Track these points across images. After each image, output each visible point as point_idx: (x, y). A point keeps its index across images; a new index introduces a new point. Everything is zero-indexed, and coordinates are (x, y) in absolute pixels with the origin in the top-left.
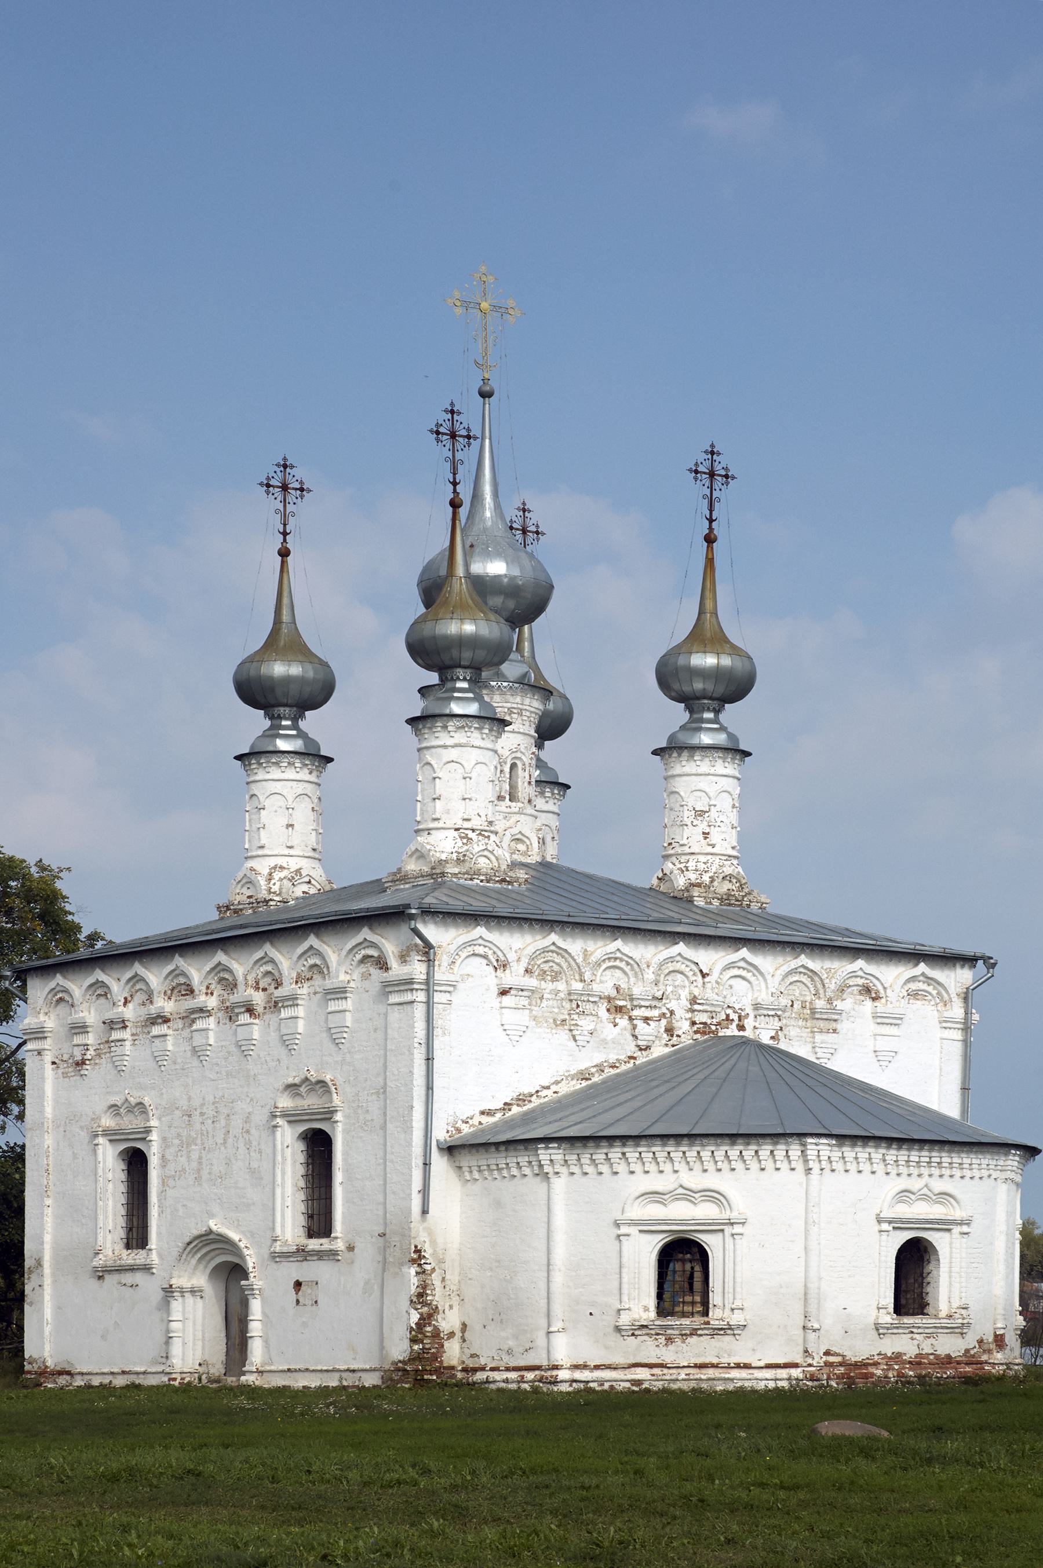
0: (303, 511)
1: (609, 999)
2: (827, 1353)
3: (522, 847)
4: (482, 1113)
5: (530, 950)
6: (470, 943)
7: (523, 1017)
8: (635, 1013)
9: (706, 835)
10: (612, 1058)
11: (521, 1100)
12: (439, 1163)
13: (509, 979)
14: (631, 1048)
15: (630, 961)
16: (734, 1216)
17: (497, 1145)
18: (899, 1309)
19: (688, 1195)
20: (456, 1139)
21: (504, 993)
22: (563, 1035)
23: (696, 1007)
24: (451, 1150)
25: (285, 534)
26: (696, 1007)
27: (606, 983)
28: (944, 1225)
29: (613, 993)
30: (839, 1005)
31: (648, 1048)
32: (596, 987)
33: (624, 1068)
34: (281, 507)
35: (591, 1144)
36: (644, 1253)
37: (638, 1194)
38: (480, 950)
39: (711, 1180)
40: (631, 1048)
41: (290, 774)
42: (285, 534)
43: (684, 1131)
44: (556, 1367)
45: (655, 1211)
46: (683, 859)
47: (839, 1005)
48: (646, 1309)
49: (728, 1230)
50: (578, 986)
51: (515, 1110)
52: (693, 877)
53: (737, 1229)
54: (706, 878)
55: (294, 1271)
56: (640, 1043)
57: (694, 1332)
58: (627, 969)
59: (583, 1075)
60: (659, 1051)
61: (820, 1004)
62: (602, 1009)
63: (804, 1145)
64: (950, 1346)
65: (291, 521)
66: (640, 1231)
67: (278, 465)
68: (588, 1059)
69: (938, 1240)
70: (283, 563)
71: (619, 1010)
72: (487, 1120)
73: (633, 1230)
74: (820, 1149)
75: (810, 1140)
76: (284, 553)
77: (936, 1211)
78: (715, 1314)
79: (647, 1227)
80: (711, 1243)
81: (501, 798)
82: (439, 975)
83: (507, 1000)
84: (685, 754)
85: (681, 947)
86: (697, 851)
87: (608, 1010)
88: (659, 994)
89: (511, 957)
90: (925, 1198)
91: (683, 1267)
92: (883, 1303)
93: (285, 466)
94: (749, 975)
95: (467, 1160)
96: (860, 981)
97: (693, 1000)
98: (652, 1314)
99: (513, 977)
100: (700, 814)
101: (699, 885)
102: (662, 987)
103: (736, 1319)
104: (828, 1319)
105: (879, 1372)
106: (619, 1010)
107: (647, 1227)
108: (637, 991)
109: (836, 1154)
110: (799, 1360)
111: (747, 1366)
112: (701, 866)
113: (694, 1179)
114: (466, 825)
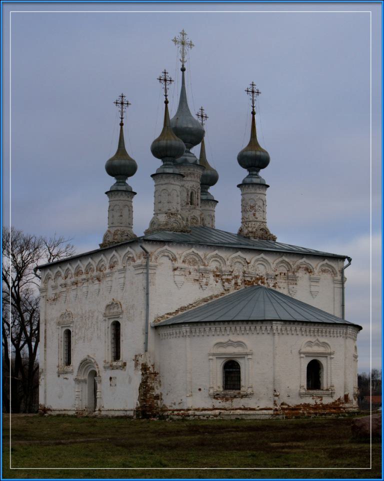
0: (127, 110)
1: (214, 272)
2: (282, 404)
3: (195, 221)
4: (168, 314)
5: (184, 254)
6: (163, 252)
7: (182, 278)
8: (224, 277)
9: (254, 215)
10: (216, 293)
11: (182, 309)
12: (151, 333)
13: (176, 265)
14: (222, 290)
15: (221, 258)
16: (248, 351)
17: (169, 325)
18: (310, 387)
19: (230, 344)
20: (157, 324)
21: (175, 269)
22: (197, 286)
23: (246, 275)
24: (156, 328)
25: (122, 118)
26: (246, 275)
27: (213, 266)
28: (325, 355)
29: (215, 270)
30: (297, 274)
31: (228, 290)
32: (208, 268)
33: (220, 297)
34: (121, 110)
35: (199, 325)
36: (218, 367)
37: (214, 344)
38: (166, 254)
39: (240, 338)
40: (222, 290)
41: (122, 198)
42: (122, 118)
43: (230, 319)
44: (188, 410)
45: (222, 350)
46: (247, 223)
47: (297, 274)
48: (219, 387)
49: (246, 357)
50: (202, 267)
51: (180, 313)
52: (250, 229)
53: (250, 357)
54: (254, 230)
55: (110, 373)
56: (226, 288)
57: (235, 397)
58: (220, 261)
59: (205, 300)
60: (232, 291)
61: (290, 274)
62: (211, 276)
63: (272, 324)
64: (327, 401)
65: (124, 114)
66: (217, 358)
67: (120, 96)
68: (206, 294)
69: (323, 361)
70: (122, 128)
71: (217, 276)
72: (171, 317)
73: (214, 358)
74: (277, 326)
75: (274, 322)
76: (122, 124)
77: (321, 350)
78: (242, 389)
79: (218, 356)
80: (241, 362)
81: (187, 204)
82: (150, 263)
83: (177, 272)
84: (247, 186)
85: (239, 253)
86: (251, 219)
87: (214, 276)
88: (232, 270)
89: (177, 256)
90: (317, 345)
91: (232, 372)
92: (302, 384)
93: (122, 97)
94: (265, 264)
95: (163, 332)
96: (304, 266)
97: (244, 273)
98: (221, 389)
99: (179, 264)
100: (252, 207)
101: (252, 232)
102: (233, 267)
103: (249, 391)
104: (282, 393)
105: (301, 411)
106: (217, 276)
107: (218, 356)
108: (223, 269)
109: (284, 328)
110: (272, 406)
111: (254, 409)
112: (253, 226)
113: (234, 338)
114: (169, 212)
